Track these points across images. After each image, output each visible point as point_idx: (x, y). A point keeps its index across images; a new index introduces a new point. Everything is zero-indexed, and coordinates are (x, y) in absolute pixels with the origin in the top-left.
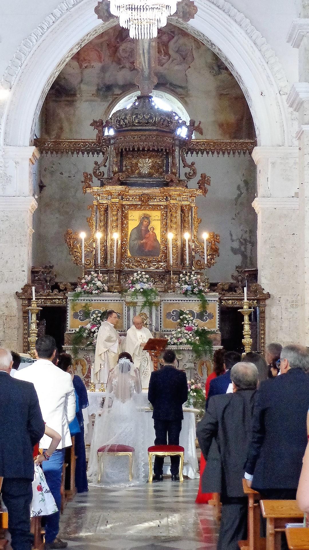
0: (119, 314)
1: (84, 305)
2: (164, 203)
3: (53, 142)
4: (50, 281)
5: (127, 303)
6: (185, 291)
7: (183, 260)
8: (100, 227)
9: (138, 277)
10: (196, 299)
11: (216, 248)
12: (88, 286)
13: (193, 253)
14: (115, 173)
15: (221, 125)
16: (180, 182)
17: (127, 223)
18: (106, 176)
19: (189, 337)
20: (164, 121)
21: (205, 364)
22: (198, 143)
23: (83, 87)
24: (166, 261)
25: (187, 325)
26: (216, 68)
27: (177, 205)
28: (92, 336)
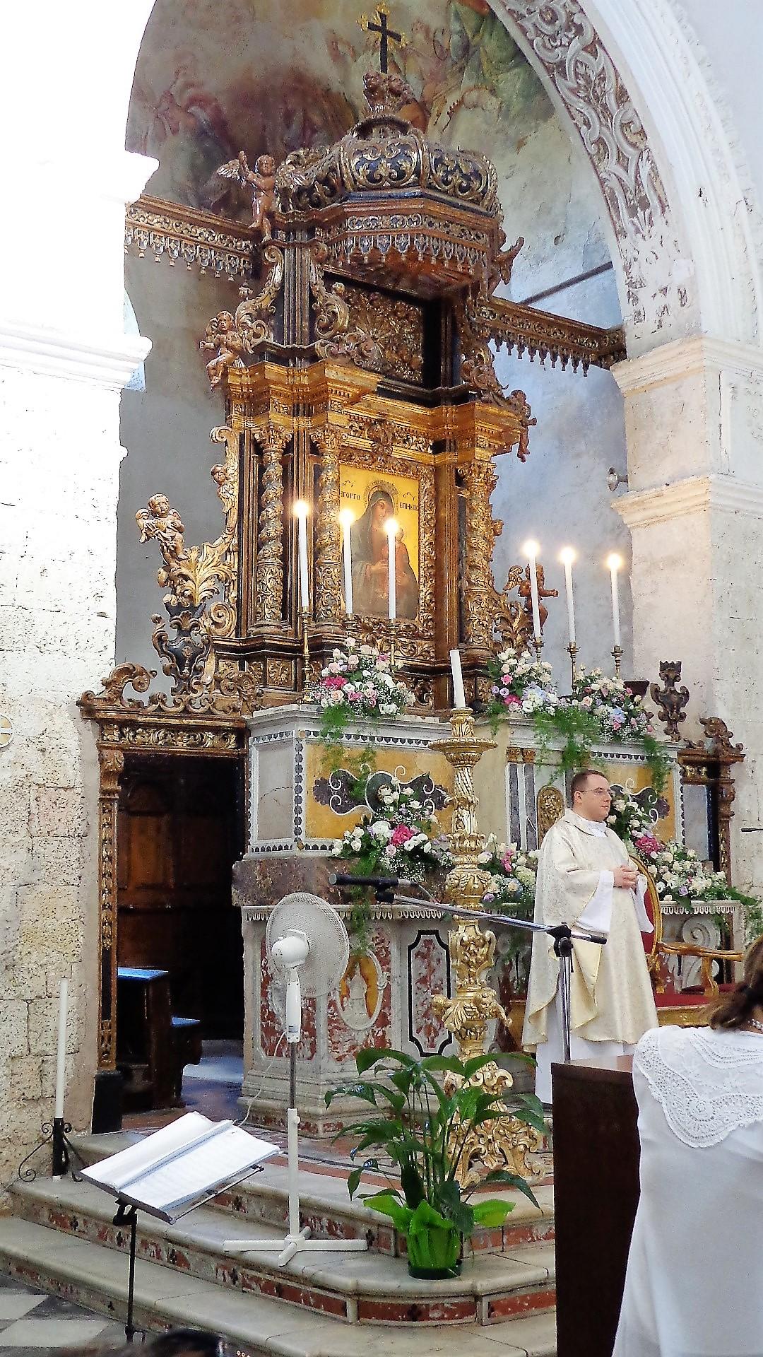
0: (445, 790)
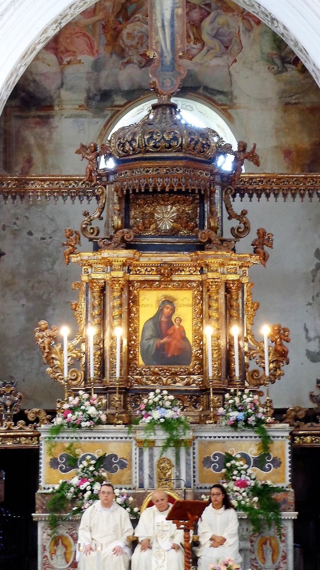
0: (126, 460)
1: (67, 445)
2: (197, 277)
3: (16, 180)
4: (11, 406)
5: (140, 443)
7: (229, 370)
8: (93, 317)
10: (253, 434)
11: (284, 351)
12: (73, 413)
14: (116, 229)
15: (287, 153)
17: (138, 310)
18: (101, 235)
19: (241, 498)
20: (197, 143)
21: (268, 543)
22: (251, 179)
23: (64, 94)
24: (202, 371)
25: (238, 478)
26: (278, 62)
27: (219, 280)
28: (81, 498)
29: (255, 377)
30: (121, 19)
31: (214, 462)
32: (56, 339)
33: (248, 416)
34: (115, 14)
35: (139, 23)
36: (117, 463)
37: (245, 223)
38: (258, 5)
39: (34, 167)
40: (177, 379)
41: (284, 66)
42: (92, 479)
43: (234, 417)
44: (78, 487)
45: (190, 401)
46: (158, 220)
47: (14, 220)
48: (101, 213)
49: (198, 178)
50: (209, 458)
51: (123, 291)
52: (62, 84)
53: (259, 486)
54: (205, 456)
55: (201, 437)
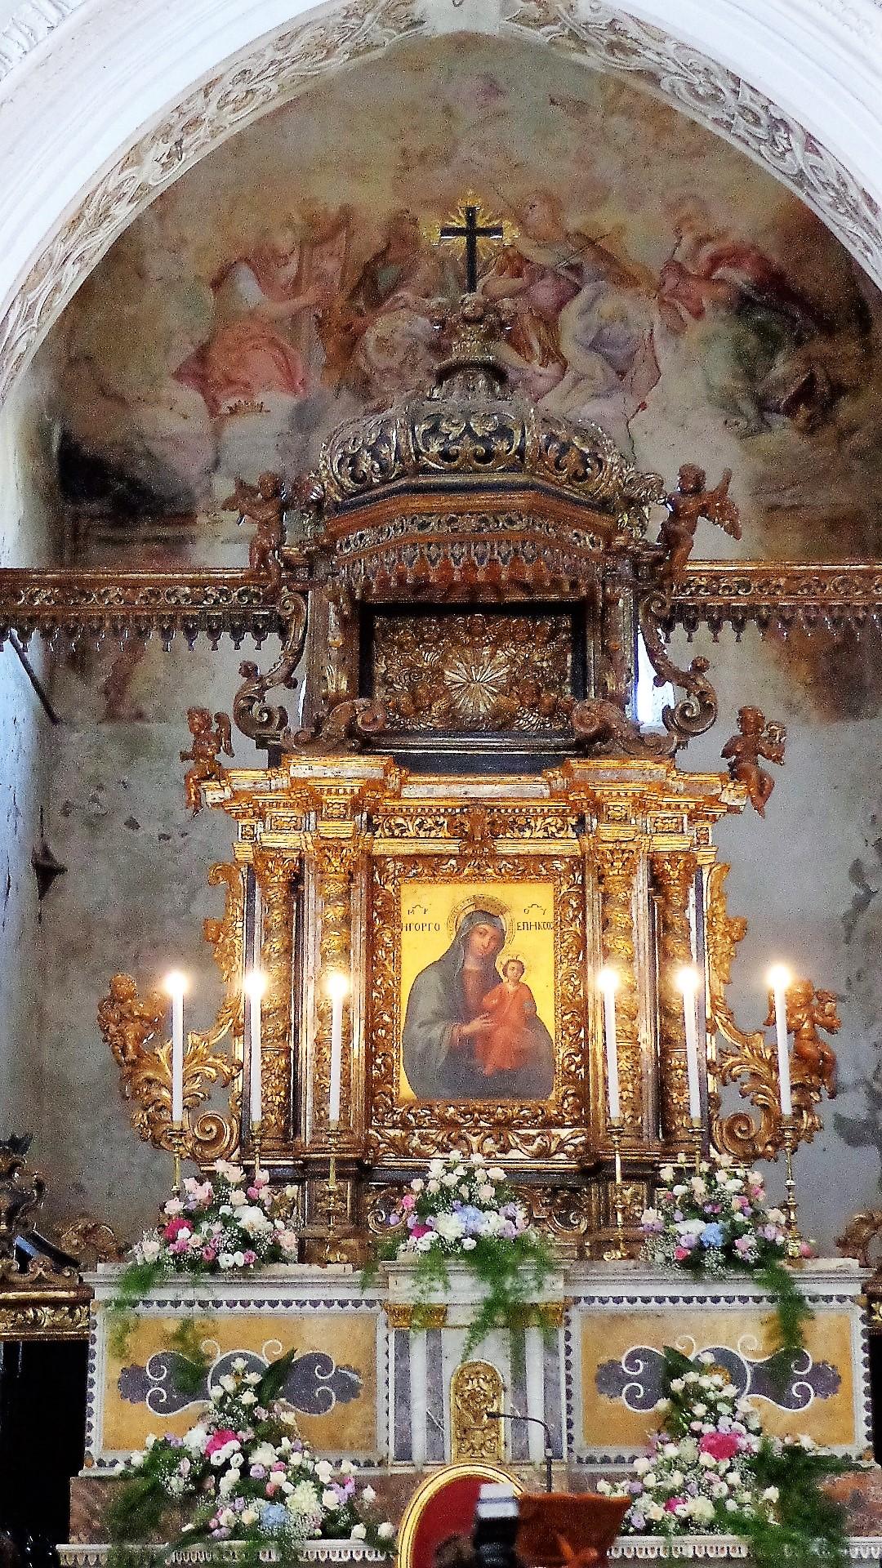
0: (357, 1372)
1: (172, 1327)
2: (566, 845)
3: (55, 584)
5: (398, 1314)
6: (690, 1249)
7: (664, 1110)
8: (268, 959)
9: (451, 1180)
10: (751, 1290)
12: (194, 1228)
13: (712, 1085)
14: (333, 701)
16: (639, 743)
17: (396, 940)
18: (294, 725)
19: (726, 1490)
20: (565, 448)
22: (716, 577)
25: (708, 1429)
26: (748, 408)
27: (632, 846)
28: (213, 1492)
29: (739, 1135)
30: (361, 303)
31: (629, 1379)
32: (157, 1024)
33: (736, 1232)
34: (346, 293)
35: (404, 312)
36: (329, 1383)
37: (702, 695)
38: (732, 85)
39: (144, 660)
40: (513, 1139)
41: (763, 419)
42: (248, 1434)
43: (693, 1237)
44: (205, 1457)
45: (550, 1204)
46: (454, 687)
47: (93, 792)
48: (292, 668)
49: (568, 548)
50: (614, 1364)
51: (351, 880)
52: (217, 463)
53: (777, 1452)
54: (604, 1360)
55: (591, 1299)
